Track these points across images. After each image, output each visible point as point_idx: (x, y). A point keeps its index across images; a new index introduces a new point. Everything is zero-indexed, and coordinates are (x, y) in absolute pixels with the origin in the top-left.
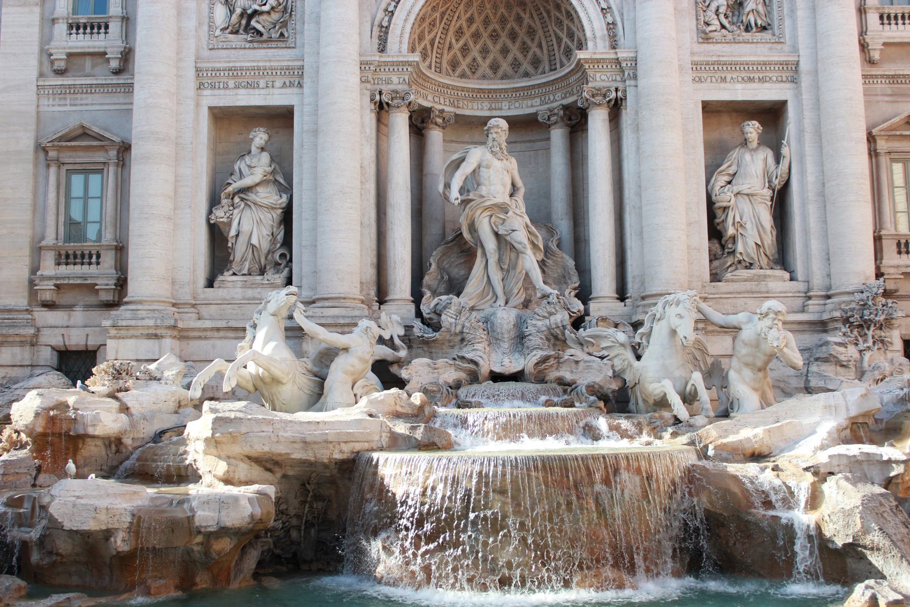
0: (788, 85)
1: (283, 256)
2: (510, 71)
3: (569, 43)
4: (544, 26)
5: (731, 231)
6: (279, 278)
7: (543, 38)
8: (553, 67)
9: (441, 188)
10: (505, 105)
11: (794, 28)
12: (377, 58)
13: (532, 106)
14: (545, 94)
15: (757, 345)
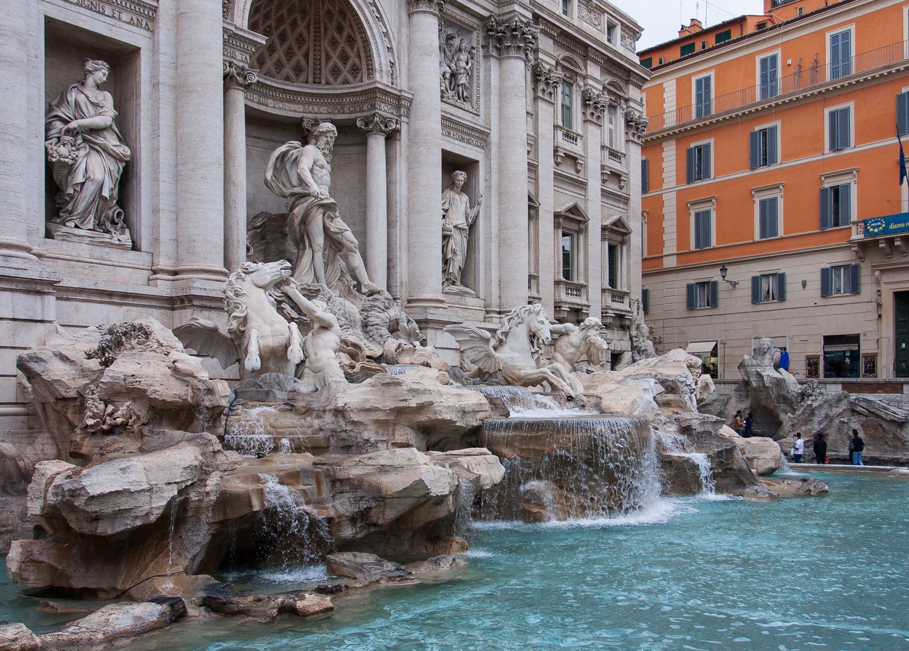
0: (480, 150)
1: (119, 214)
2: (274, 72)
3: (340, 64)
4: (317, 39)
5: (450, 255)
6: (126, 238)
7: (311, 50)
8: (318, 80)
9: (269, 175)
10: (270, 102)
11: (488, 107)
12: (233, 29)
13: (295, 111)
14: (309, 104)
15: (577, 348)
